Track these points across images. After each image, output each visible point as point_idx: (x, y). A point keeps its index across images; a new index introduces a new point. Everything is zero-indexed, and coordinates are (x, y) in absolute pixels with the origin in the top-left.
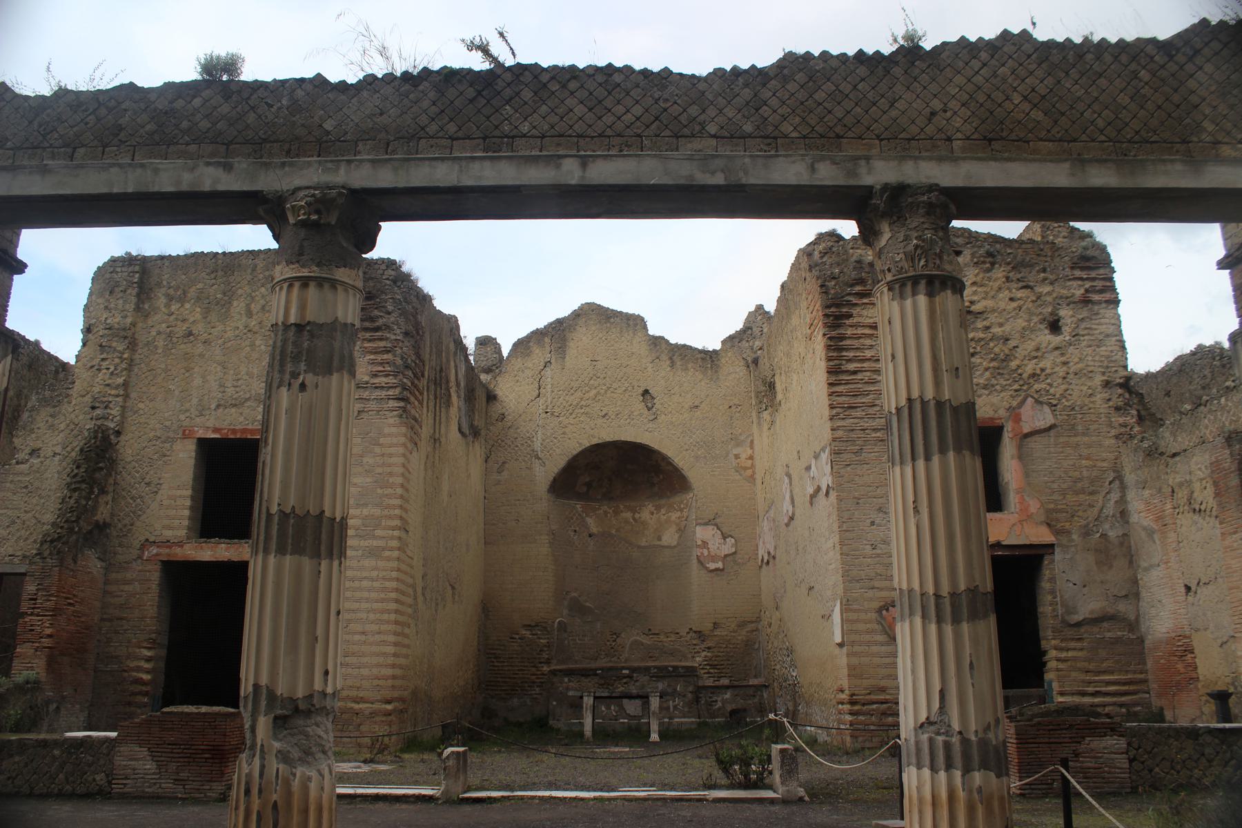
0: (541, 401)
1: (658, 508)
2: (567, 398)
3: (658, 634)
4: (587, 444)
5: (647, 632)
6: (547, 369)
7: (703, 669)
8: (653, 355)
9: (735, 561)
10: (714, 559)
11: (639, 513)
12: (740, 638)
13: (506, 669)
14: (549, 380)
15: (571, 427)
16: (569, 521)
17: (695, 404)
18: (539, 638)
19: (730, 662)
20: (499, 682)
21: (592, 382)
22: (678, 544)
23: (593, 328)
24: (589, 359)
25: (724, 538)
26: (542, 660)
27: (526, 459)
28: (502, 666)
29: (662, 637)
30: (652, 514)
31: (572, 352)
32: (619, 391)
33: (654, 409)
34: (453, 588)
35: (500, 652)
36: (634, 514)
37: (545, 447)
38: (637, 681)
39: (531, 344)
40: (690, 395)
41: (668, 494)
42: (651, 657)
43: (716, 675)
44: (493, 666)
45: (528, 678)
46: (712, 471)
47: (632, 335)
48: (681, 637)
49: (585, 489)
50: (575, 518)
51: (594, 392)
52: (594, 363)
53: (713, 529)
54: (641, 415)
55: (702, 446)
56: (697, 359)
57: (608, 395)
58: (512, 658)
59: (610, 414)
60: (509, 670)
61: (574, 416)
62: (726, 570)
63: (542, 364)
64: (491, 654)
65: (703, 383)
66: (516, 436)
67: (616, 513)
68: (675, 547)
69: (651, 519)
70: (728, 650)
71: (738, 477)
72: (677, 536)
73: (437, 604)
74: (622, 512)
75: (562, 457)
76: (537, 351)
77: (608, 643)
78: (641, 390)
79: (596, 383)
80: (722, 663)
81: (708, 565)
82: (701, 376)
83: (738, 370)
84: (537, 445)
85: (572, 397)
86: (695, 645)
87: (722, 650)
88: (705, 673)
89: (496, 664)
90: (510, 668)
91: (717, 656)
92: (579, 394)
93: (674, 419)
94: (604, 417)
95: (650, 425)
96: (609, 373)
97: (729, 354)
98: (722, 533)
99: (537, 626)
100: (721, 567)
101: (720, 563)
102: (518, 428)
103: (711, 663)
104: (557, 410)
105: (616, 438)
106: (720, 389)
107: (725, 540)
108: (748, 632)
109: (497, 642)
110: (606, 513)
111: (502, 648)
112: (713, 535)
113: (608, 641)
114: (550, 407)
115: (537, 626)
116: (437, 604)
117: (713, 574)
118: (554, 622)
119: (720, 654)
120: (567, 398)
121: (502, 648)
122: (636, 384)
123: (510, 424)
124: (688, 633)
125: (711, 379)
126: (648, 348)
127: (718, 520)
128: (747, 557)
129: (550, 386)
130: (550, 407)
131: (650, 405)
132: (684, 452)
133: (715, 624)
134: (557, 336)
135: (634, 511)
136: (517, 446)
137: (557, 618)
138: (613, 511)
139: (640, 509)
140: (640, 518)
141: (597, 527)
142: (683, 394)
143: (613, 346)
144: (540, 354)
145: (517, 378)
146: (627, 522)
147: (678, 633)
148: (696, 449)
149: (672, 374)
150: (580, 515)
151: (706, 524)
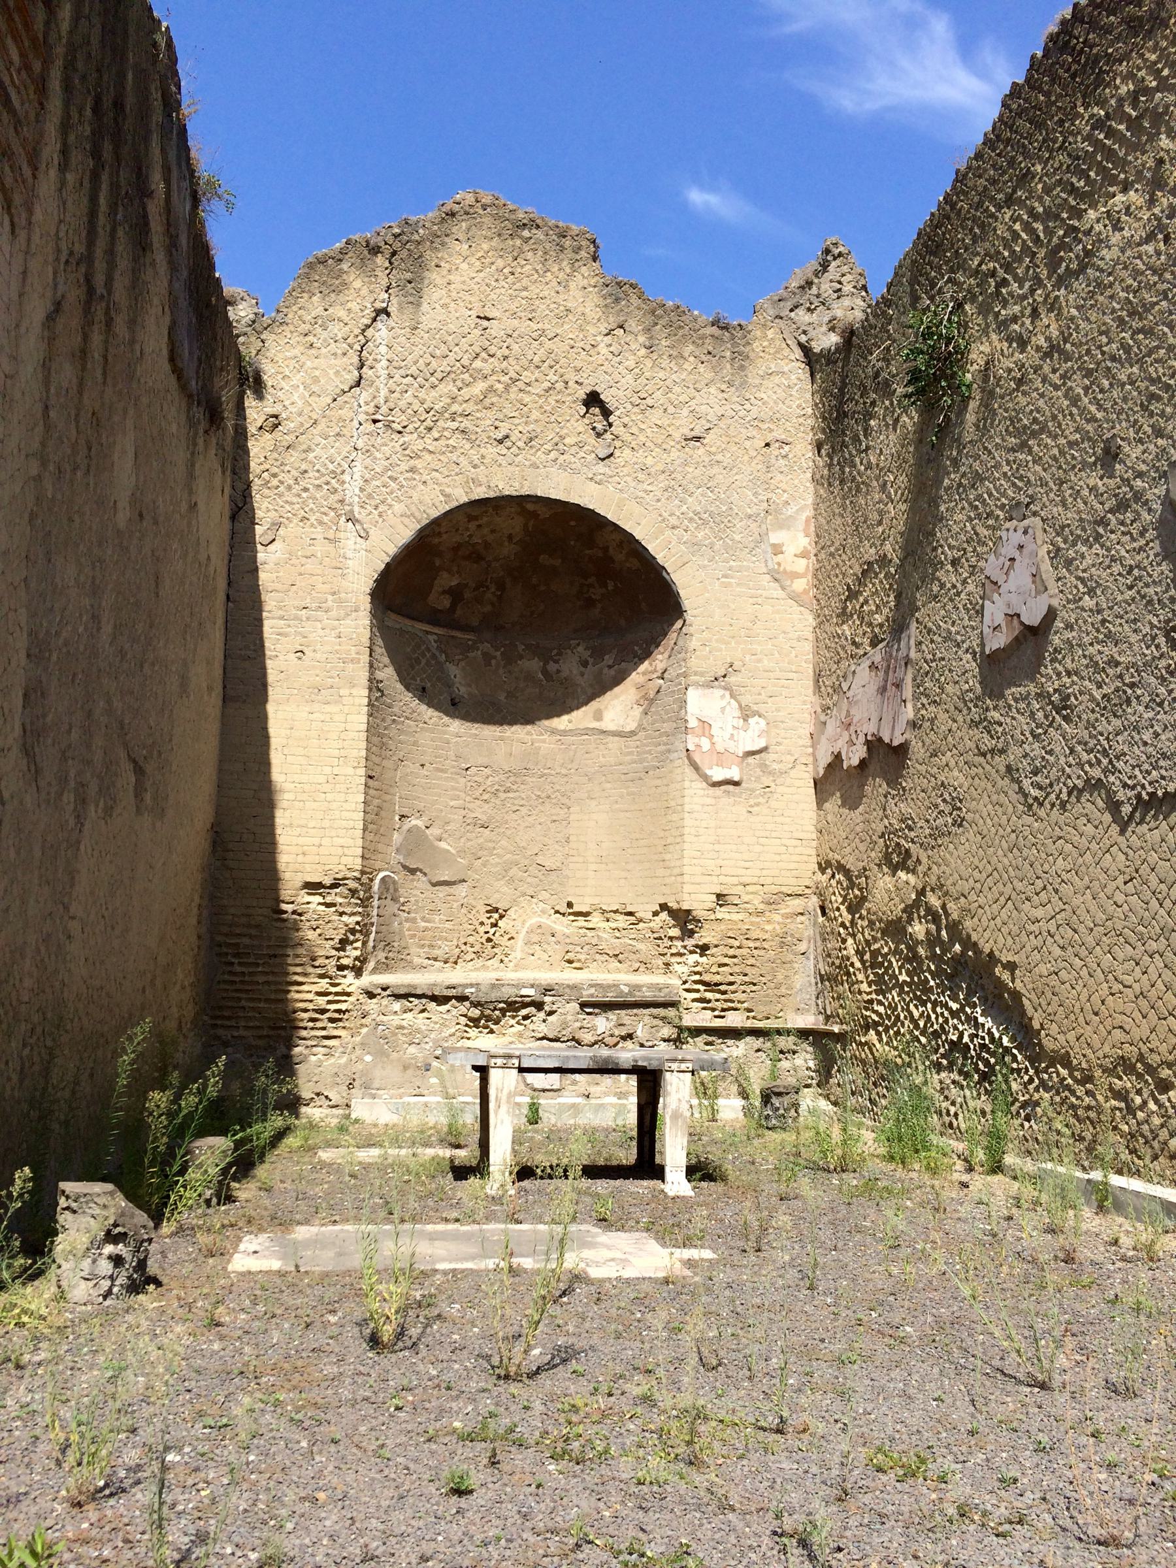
0: (364, 395)
1: (598, 653)
2: (422, 394)
3: (587, 914)
4: (461, 496)
5: (564, 909)
6: (379, 325)
7: (687, 990)
8: (611, 319)
9: (763, 766)
10: (721, 757)
11: (556, 662)
12: (768, 927)
13: (261, 979)
14: (383, 349)
15: (428, 457)
16: (413, 667)
17: (696, 433)
18: (341, 914)
19: (746, 979)
20: (243, 1008)
21: (478, 364)
22: (641, 727)
23: (485, 246)
24: (474, 313)
25: (746, 714)
26: (345, 961)
27: (325, 519)
28: (251, 974)
29: (596, 920)
30: (585, 664)
31: (434, 296)
32: (537, 389)
33: (608, 436)
34: (139, 770)
35: (246, 941)
36: (546, 663)
37: (370, 496)
38: (551, 1013)
39: (345, 266)
40: (685, 412)
41: (623, 622)
42: (570, 962)
43: (719, 1005)
44: (230, 973)
45: (311, 1001)
46: (725, 576)
47: (568, 270)
48: (641, 920)
49: (446, 602)
50: (424, 661)
51: (480, 386)
52: (485, 323)
53: (723, 697)
54: (580, 445)
55: (705, 522)
56: (703, 337)
57: (512, 396)
58: (275, 956)
59: (513, 438)
60: (267, 983)
61: (437, 435)
62: (743, 785)
63: (369, 312)
64: (229, 945)
65: (713, 390)
66: (304, 467)
67: (510, 659)
68: (633, 733)
69: (582, 674)
70: (744, 951)
71: (780, 593)
72: (638, 711)
73: (83, 801)
74: (521, 657)
75: (406, 521)
76: (357, 284)
77: (482, 929)
78: (582, 394)
79: (487, 368)
80: (732, 979)
81: (709, 772)
82: (709, 375)
83: (786, 369)
84: (352, 490)
85: (433, 393)
86: (671, 938)
87: (731, 952)
88: (694, 1000)
89: (238, 969)
90: (271, 978)
91: (721, 965)
92: (447, 388)
93: (649, 461)
94: (500, 442)
95: (601, 468)
96: (515, 347)
97: (770, 334)
98: (740, 706)
99: (334, 886)
100: (736, 779)
101: (734, 767)
102: (309, 450)
103: (707, 978)
104: (399, 419)
105: (525, 491)
106: (748, 406)
107: (745, 719)
108: (785, 916)
109: (243, 920)
110: (487, 657)
111: (253, 932)
112: (723, 709)
113: (482, 923)
114: (384, 409)
115: (334, 886)
116: (83, 801)
117: (718, 791)
118: (371, 880)
119: (726, 961)
120: (422, 394)
121: (253, 932)
122: (572, 377)
123: (290, 438)
124: (655, 914)
125: (730, 384)
126: (602, 302)
127: (732, 679)
128: (793, 759)
129: (384, 363)
130: (384, 409)
131: (599, 427)
132: (668, 532)
133: (719, 896)
134: (404, 254)
135: (546, 658)
136: (306, 490)
137: (380, 870)
138: (502, 654)
139: (560, 654)
140: (558, 671)
141: (470, 686)
142: (671, 409)
143: (525, 289)
144: (364, 292)
145: (310, 338)
146: (529, 677)
147: (631, 914)
148: (692, 526)
149: (649, 363)
150: (434, 656)
151: (708, 685)
